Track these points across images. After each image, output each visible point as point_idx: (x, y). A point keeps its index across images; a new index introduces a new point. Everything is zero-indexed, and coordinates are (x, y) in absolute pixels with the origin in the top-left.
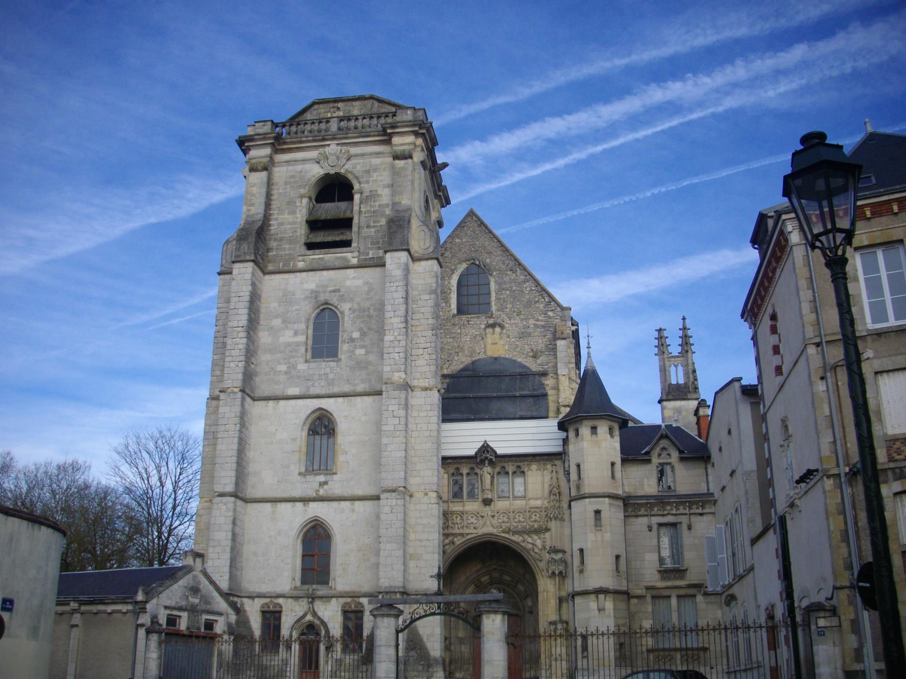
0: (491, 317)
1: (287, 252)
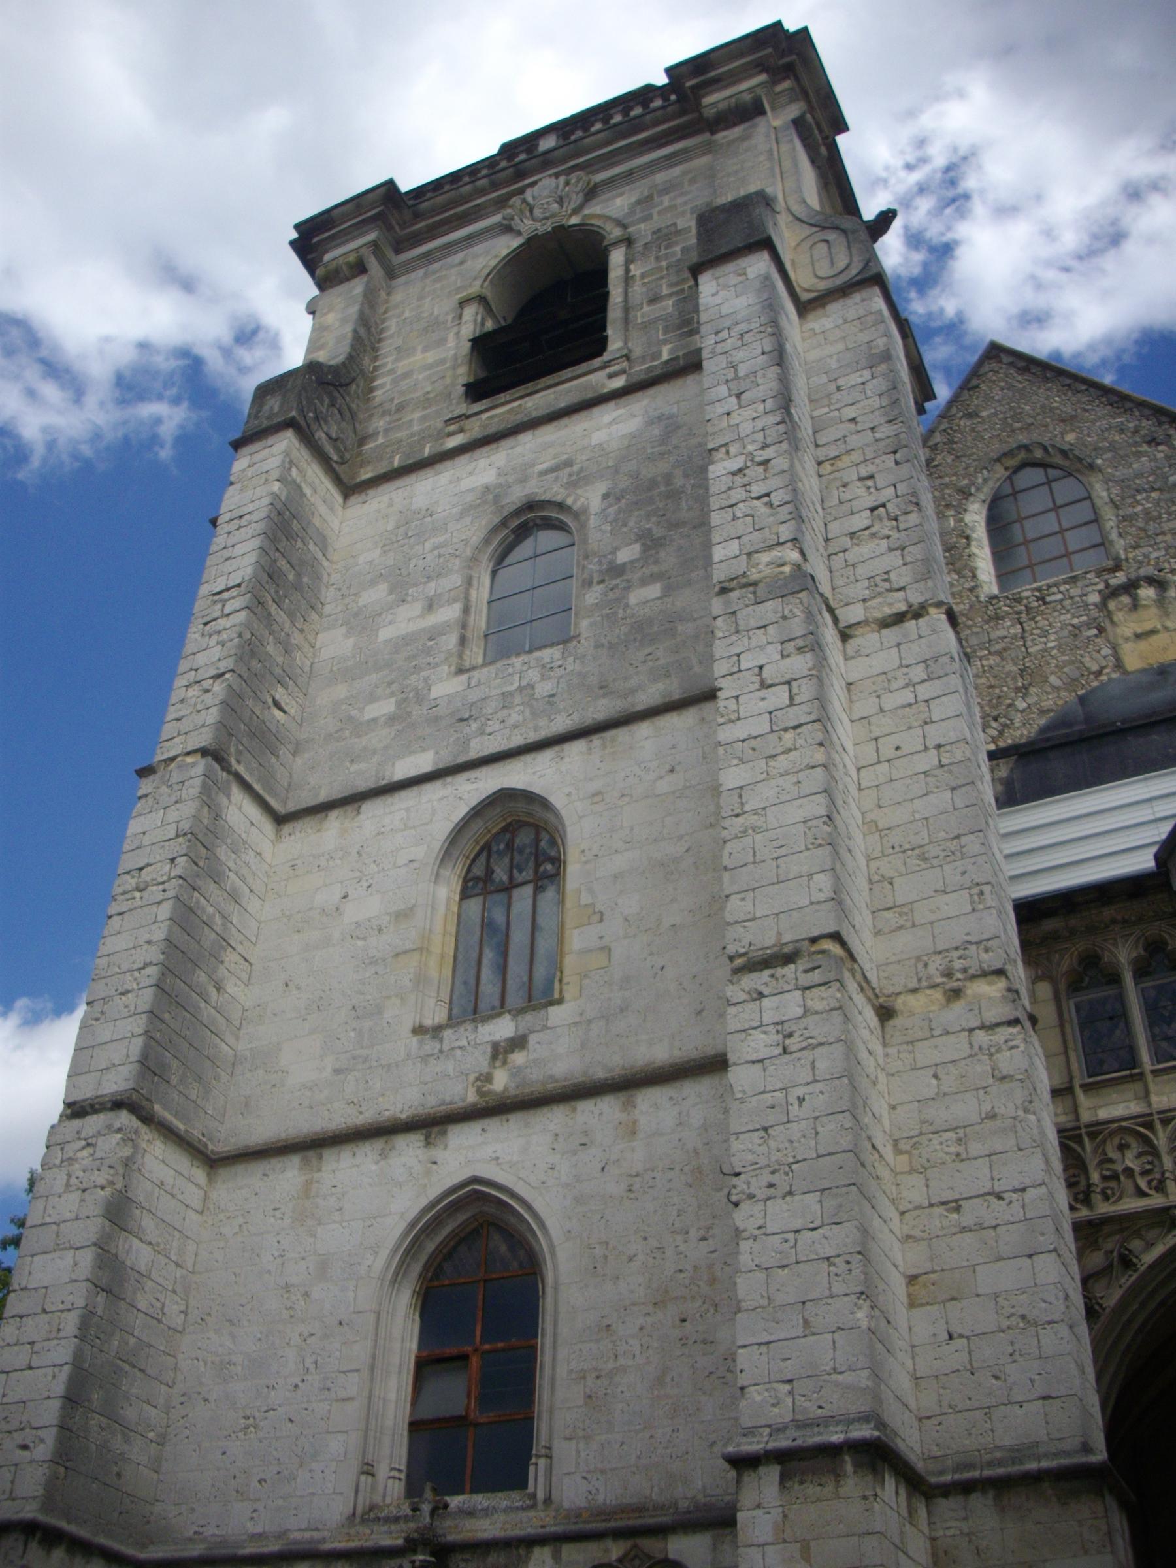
0: (1117, 568)
1: (416, 428)
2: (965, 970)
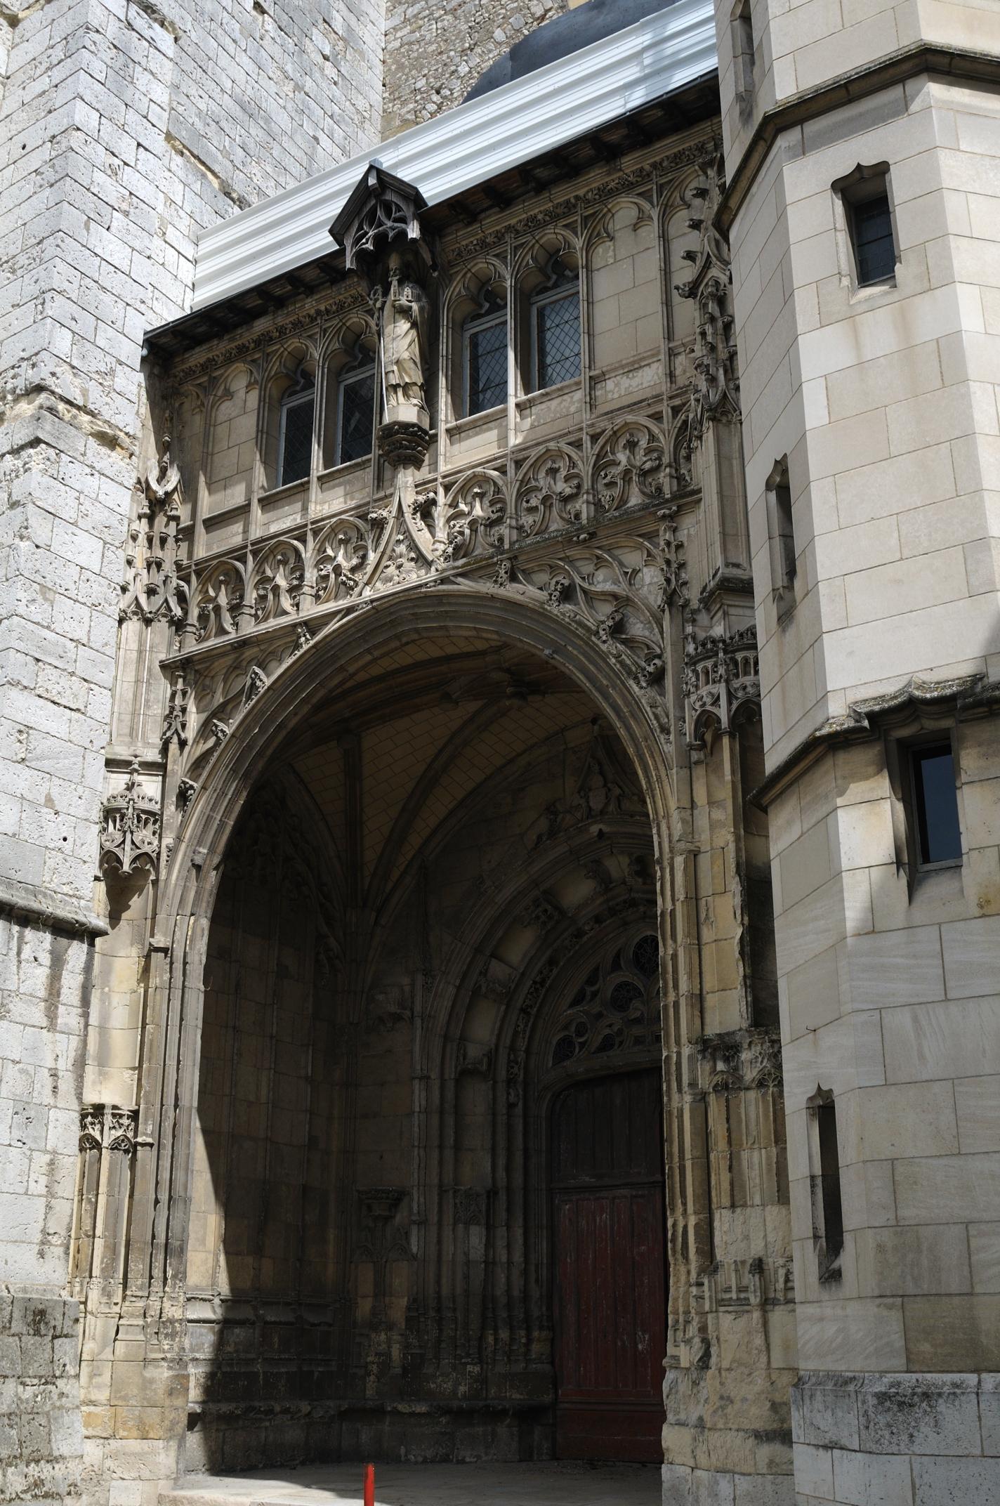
2: (13, 391)
